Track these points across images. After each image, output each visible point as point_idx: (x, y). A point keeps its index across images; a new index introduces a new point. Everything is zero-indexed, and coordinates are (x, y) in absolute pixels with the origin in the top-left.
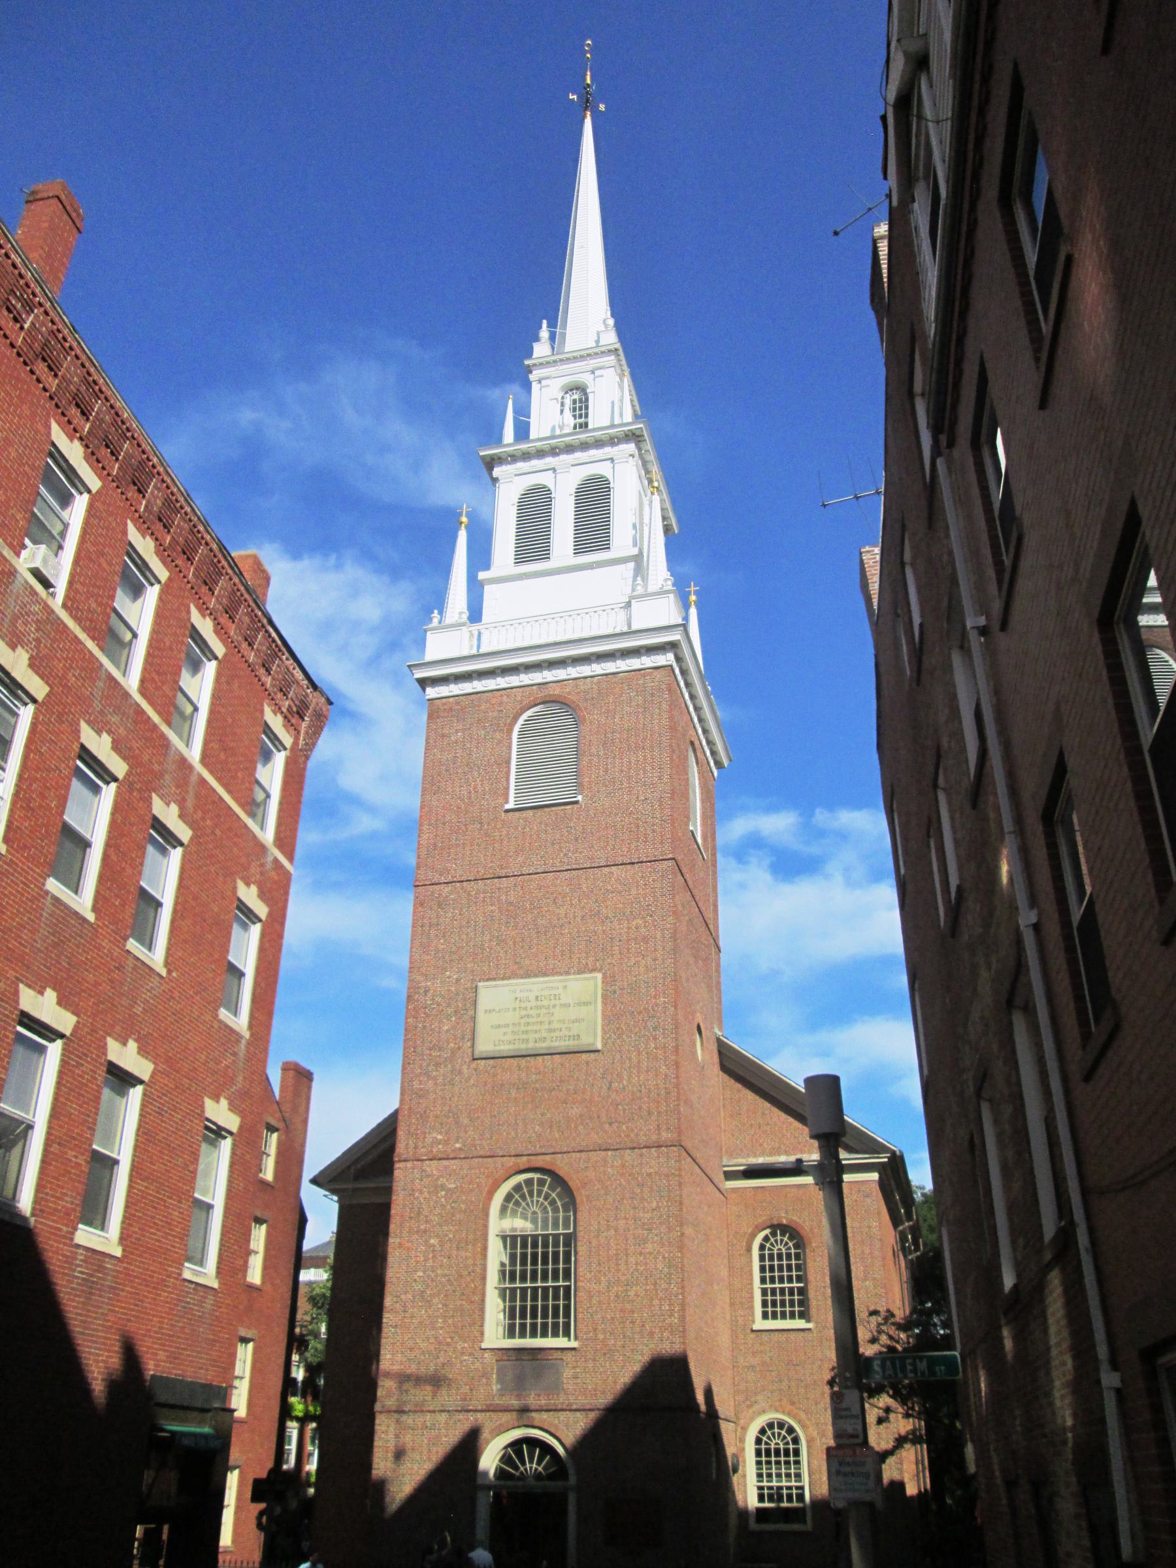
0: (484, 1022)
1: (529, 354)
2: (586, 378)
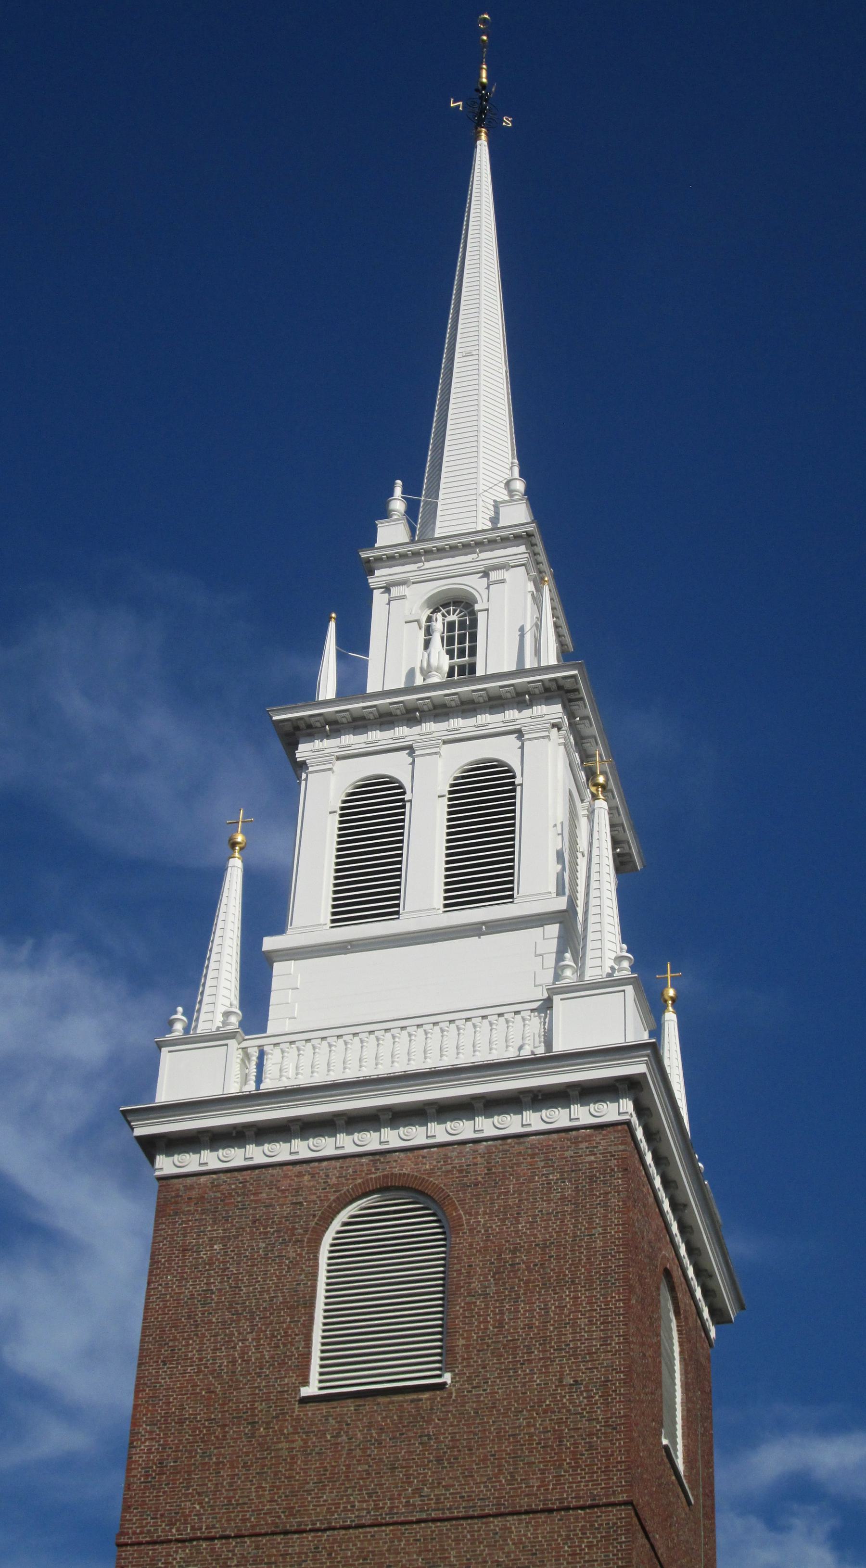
1: (370, 540)
2: (475, 585)
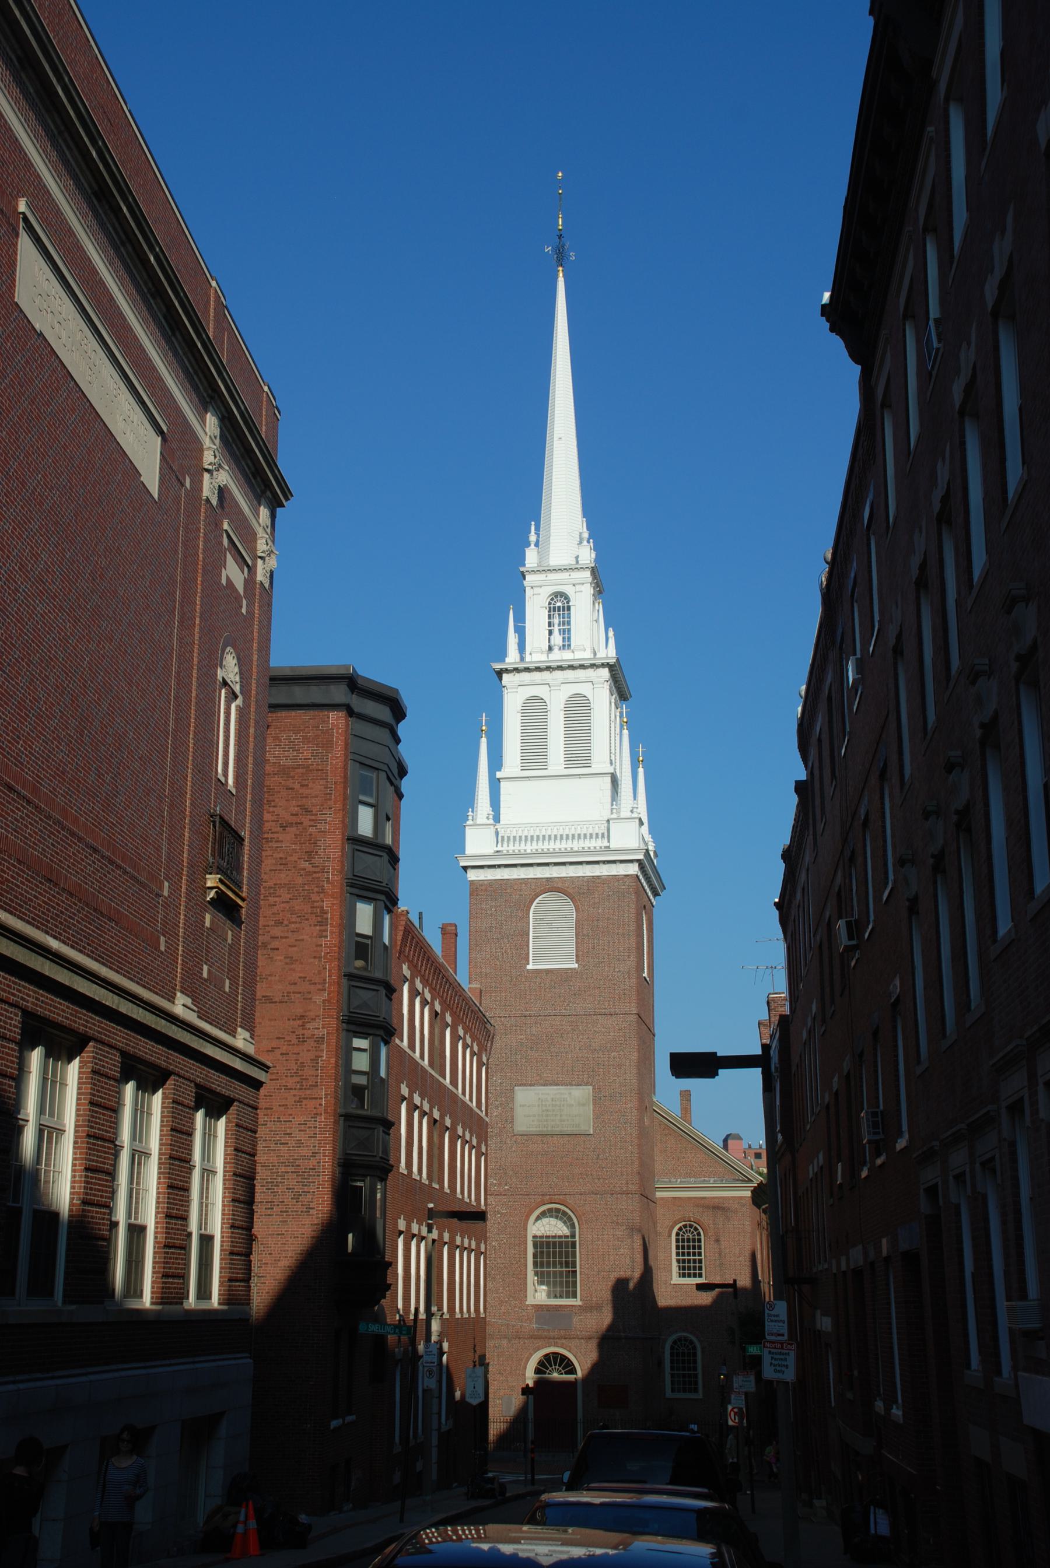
0: (520, 1113)
